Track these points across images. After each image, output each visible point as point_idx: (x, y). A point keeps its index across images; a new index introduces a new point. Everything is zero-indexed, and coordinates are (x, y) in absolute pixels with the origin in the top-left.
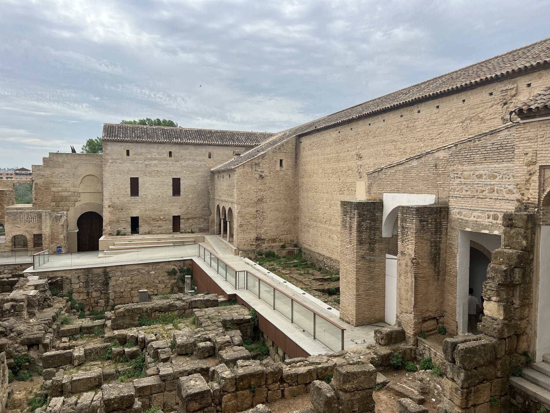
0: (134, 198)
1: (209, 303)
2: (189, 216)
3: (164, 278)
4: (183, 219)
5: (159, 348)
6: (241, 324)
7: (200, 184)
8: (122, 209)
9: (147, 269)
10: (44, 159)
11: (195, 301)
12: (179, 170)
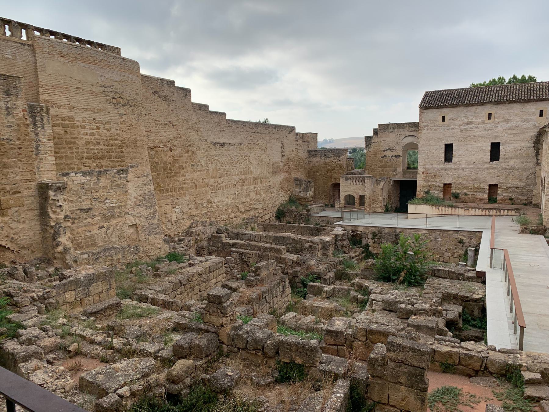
0: (448, 164)
1: (454, 275)
2: (509, 185)
3: (451, 247)
4: (501, 188)
5: (375, 300)
6: (466, 301)
7: (525, 149)
8: (435, 176)
9: (434, 235)
10: (374, 130)
11: (439, 270)
12: (500, 133)
